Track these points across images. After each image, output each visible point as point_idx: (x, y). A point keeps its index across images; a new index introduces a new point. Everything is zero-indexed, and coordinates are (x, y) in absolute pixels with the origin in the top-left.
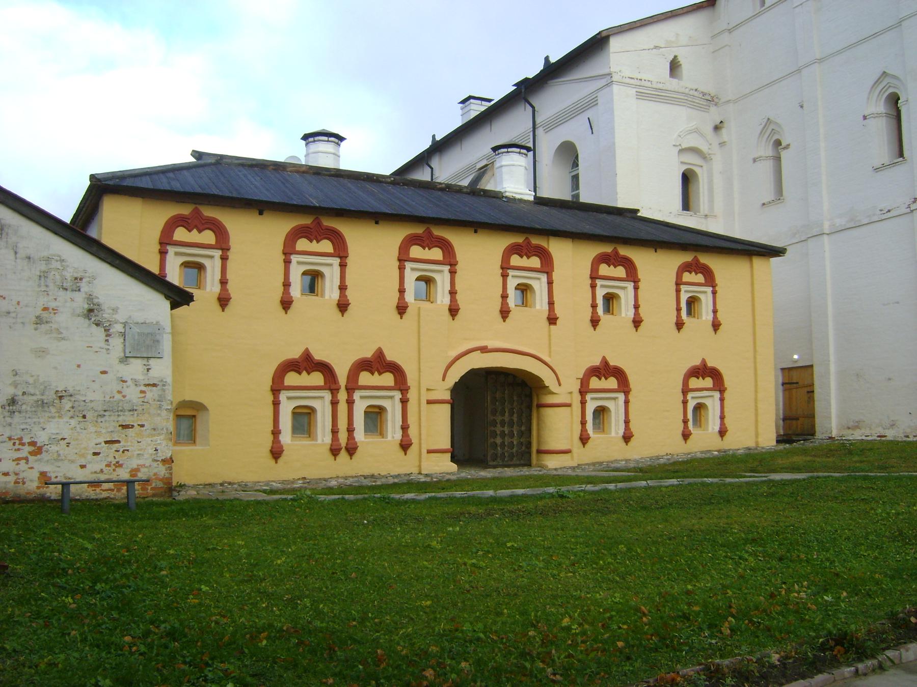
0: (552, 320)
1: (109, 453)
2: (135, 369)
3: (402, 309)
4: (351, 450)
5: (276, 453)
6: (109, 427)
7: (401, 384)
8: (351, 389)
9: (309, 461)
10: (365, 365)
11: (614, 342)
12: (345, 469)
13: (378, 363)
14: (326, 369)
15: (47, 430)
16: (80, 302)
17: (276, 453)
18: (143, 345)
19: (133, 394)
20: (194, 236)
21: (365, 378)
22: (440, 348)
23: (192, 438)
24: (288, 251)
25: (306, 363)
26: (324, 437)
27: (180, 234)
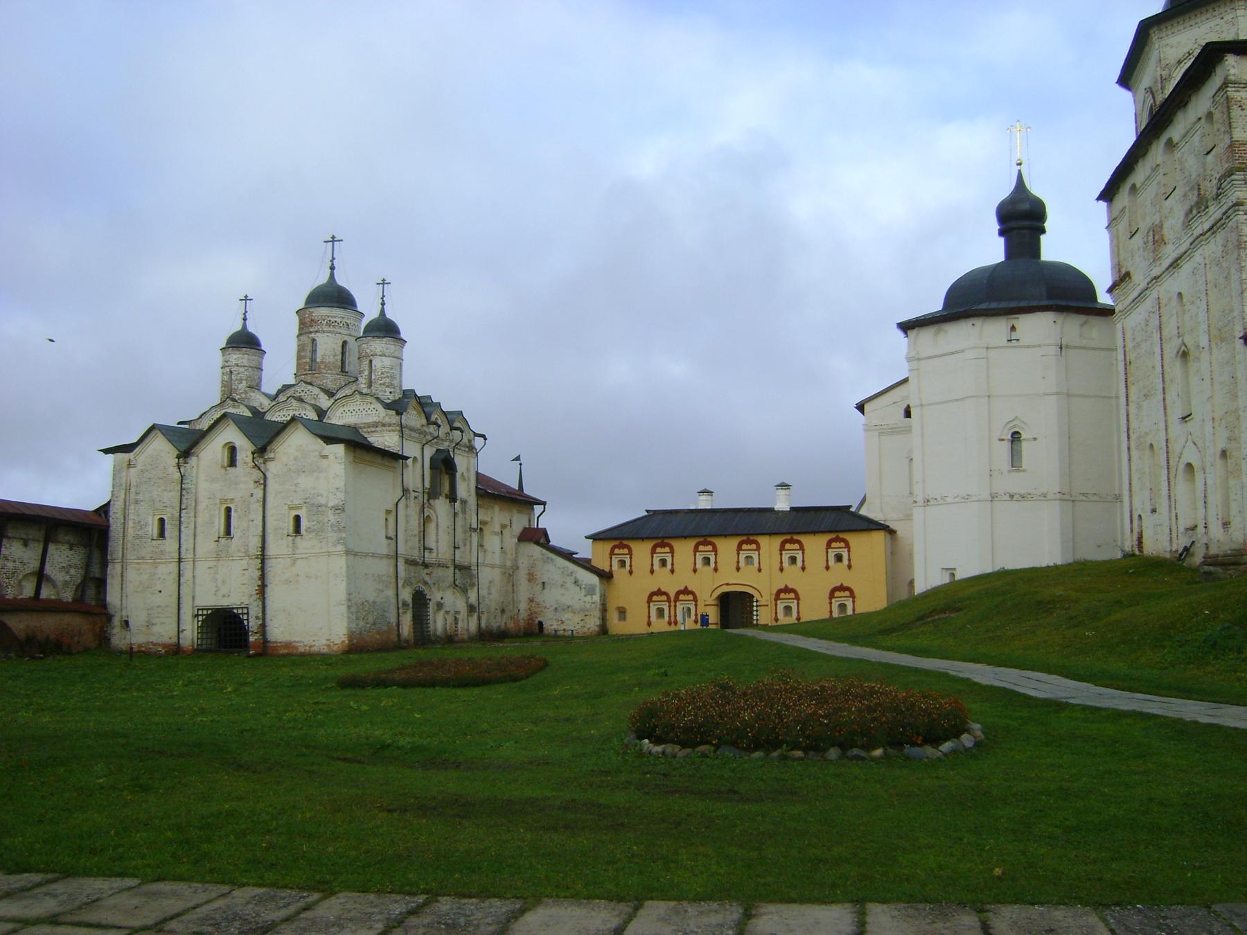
0: (760, 570)
1: (582, 623)
2: (588, 598)
3: (695, 571)
4: (676, 623)
5: (649, 624)
6: (581, 616)
7: (695, 600)
8: (677, 599)
9: (660, 626)
10: (679, 593)
11: (792, 577)
12: (673, 628)
13: (686, 591)
14: (665, 593)
15: (566, 616)
16: (572, 579)
17: (649, 624)
18: (590, 591)
19: (588, 606)
20: (621, 551)
21: (682, 597)
22: (708, 586)
23: (624, 619)
24: (653, 551)
25: (659, 592)
26: (666, 619)
27: (617, 551)
